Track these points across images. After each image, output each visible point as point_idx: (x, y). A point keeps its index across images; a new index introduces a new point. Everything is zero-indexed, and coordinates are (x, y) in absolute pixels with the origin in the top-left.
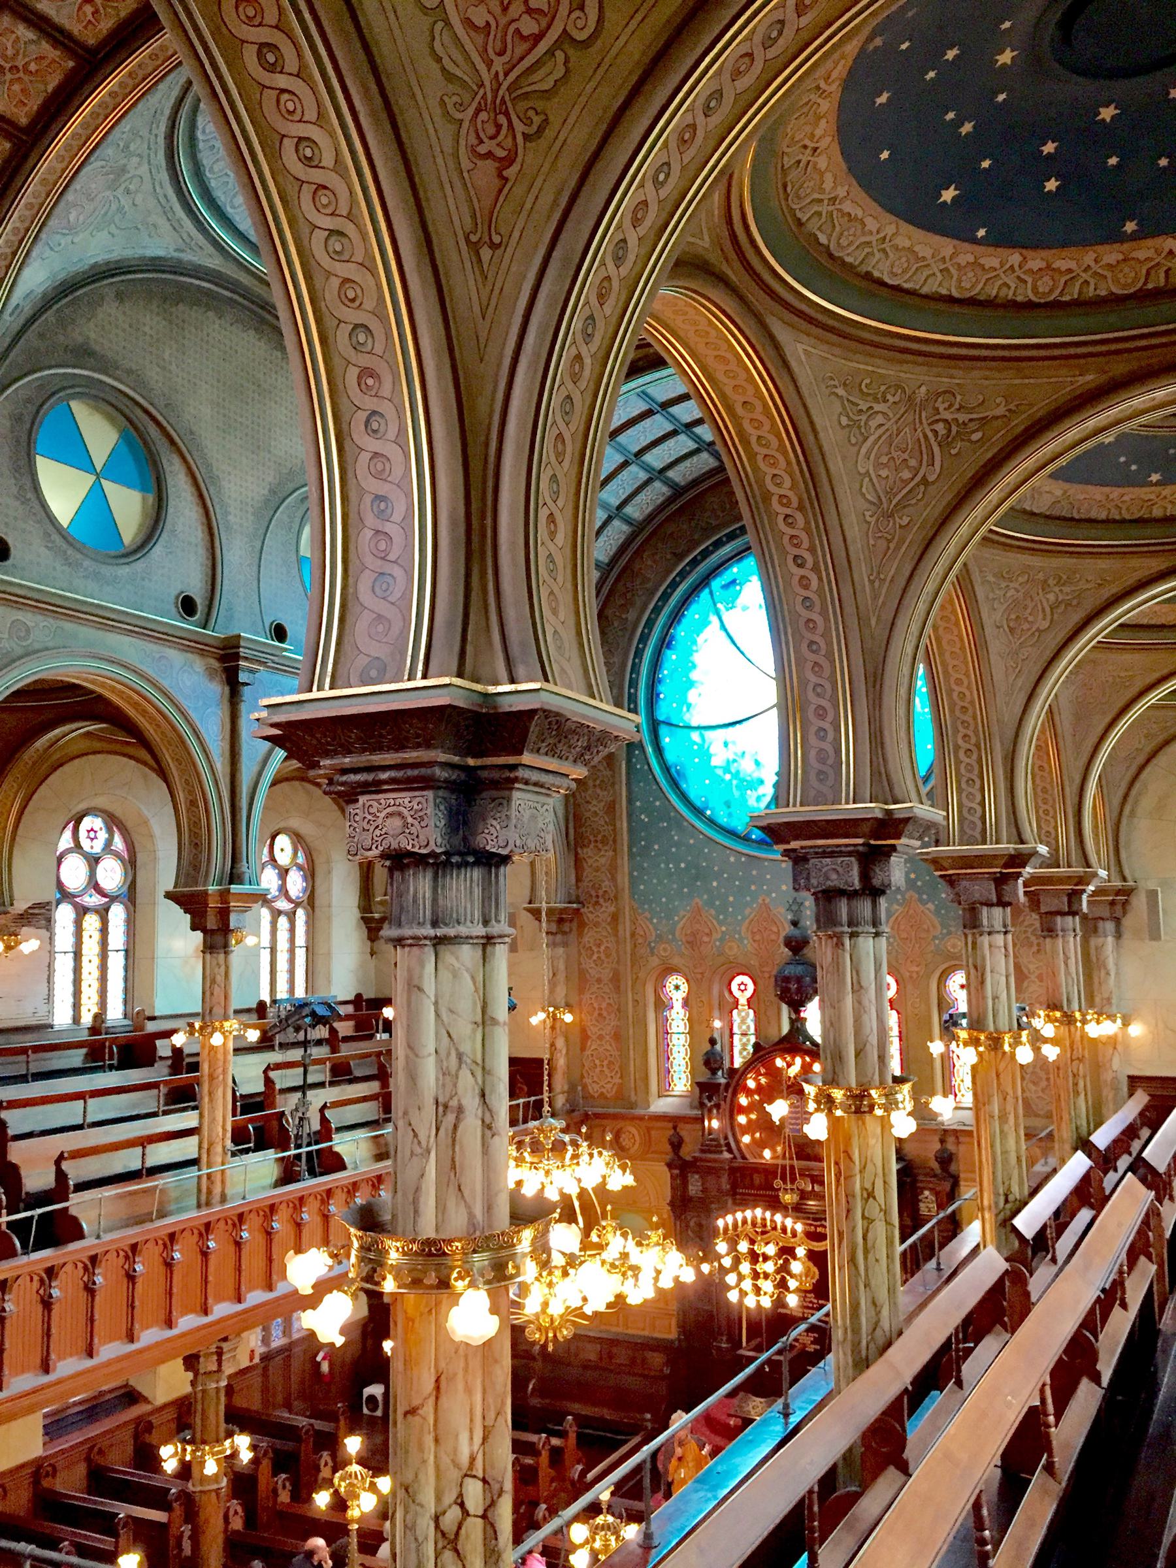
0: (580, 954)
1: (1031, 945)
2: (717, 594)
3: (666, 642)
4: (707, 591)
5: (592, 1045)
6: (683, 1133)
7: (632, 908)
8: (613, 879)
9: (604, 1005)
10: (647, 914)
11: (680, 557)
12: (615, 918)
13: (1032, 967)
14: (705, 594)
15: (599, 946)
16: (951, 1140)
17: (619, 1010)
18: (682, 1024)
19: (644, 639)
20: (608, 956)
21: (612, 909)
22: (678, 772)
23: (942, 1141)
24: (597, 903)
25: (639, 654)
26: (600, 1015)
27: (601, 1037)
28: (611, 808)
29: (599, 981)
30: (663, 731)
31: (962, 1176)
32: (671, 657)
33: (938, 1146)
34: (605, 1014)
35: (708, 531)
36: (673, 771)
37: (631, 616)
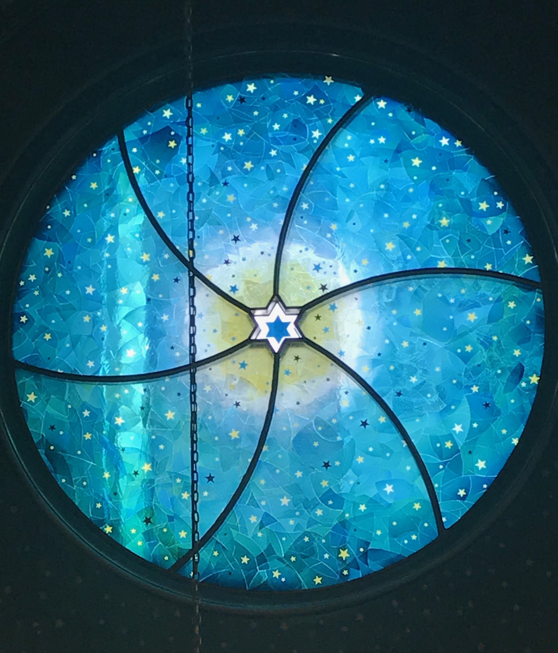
4: (114, 143)
22: (49, 453)
30: (25, 380)
36: (42, 451)
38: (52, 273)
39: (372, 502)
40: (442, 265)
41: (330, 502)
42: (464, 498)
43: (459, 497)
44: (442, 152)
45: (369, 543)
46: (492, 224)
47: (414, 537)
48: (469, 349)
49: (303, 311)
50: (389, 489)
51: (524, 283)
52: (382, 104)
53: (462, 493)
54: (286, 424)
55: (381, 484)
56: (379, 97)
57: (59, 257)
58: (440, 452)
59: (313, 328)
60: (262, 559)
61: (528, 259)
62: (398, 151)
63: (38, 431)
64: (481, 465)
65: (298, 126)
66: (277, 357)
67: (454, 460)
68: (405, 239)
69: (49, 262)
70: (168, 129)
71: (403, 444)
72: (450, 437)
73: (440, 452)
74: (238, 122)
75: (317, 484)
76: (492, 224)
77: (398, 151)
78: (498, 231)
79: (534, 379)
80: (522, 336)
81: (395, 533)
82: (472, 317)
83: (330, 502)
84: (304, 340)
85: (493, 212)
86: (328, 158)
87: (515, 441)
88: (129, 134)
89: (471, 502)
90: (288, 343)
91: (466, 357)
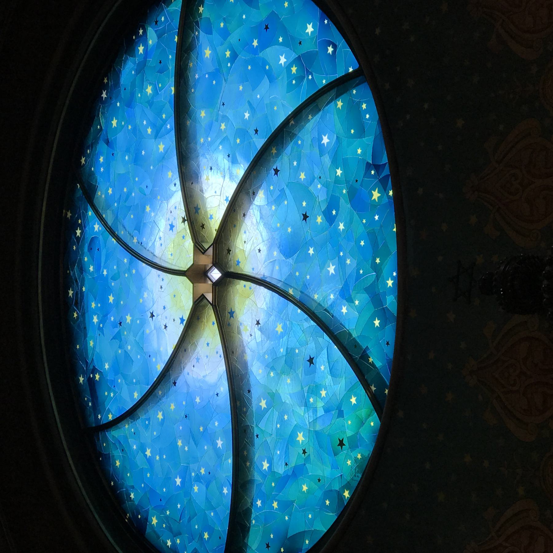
41: (334, 212)
42: (335, 47)
43: (334, 52)
45: (367, 162)
47: (364, 106)
48: (228, 54)
50: (325, 140)
53: (330, 50)
60: (376, 299)
62: (107, 142)
67: (305, 62)
71: (292, 124)
77: (107, 142)
78: (156, 31)
81: (361, 132)
83: (334, 212)
85: (144, 39)
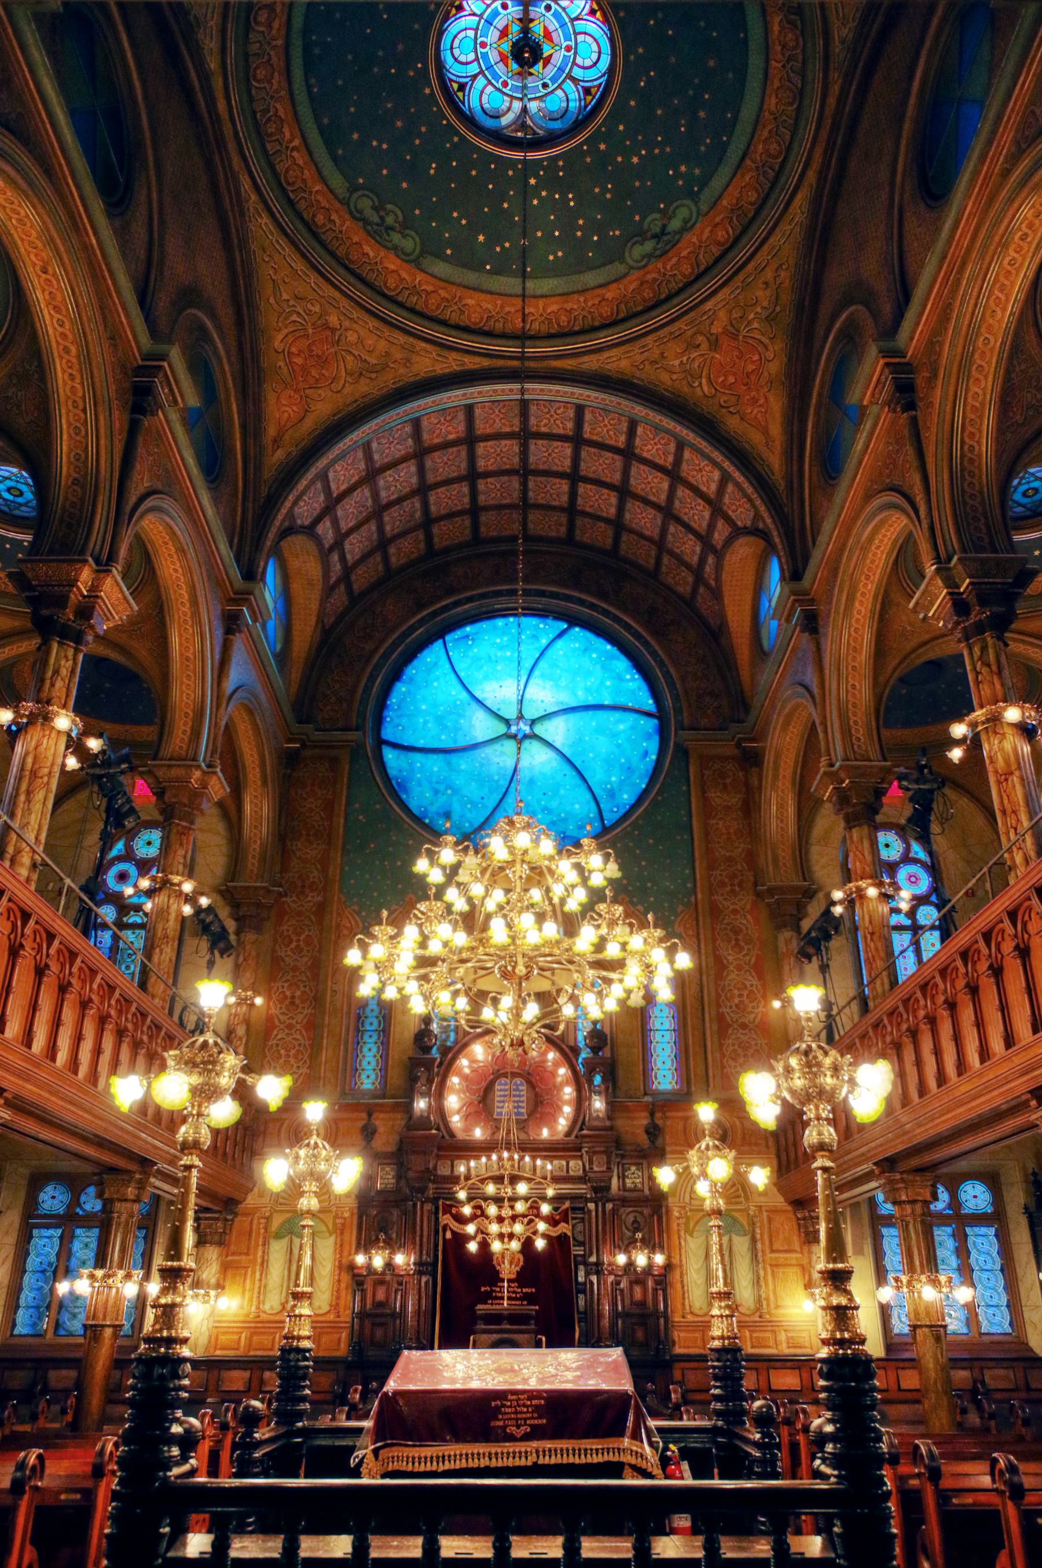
0: (275, 941)
1: (729, 941)
2: (450, 645)
3: (396, 675)
5: (279, 1034)
6: (377, 1123)
7: (339, 899)
8: (324, 870)
9: (298, 993)
10: (356, 908)
11: (421, 606)
12: (321, 909)
13: (730, 958)
14: (438, 645)
15: (299, 934)
16: (658, 1115)
17: (315, 998)
18: (375, 1022)
19: (377, 668)
20: (308, 944)
21: (320, 898)
22: (398, 783)
23: (652, 1114)
24: (303, 892)
25: (372, 679)
26: (292, 1003)
27: (290, 1027)
28: (329, 807)
29: (295, 969)
31: (668, 1149)
32: (400, 688)
33: (645, 1122)
34: (297, 1002)
35: (450, 591)
37: (369, 646)
38: (404, 699)
39: (567, 813)
40: (606, 703)
44: (607, 652)
46: (632, 685)
49: (533, 722)
51: (648, 714)
52: (577, 629)
54: (523, 775)
55: (573, 804)
56: (576, 625)
57: (409, 692)
58: (604, 790)
59: (539, 729)
61: (651, 702)
62: (585, 650)
63: (392, 772)
64: (625, 796)
65: (535, 637)
66: (520, 742)
67: (612, 794)
68: (587, 690)
69: (404, 694)
70: (467, 636)
72: (610, 783)
73: (604, 790)
74: (504, 633)
75: (539, 801)
76: (632, 685)
77: (585, 650)
79: (654, 757)
80: (648, 737)
82: (622, 727)
84: (534, 736)
85: (633, 680)
86: (549, 653)
87: (644, 786)
88: (448, 638)
89: (620, 814)
90: (526, 736)
91: (619, 746)
